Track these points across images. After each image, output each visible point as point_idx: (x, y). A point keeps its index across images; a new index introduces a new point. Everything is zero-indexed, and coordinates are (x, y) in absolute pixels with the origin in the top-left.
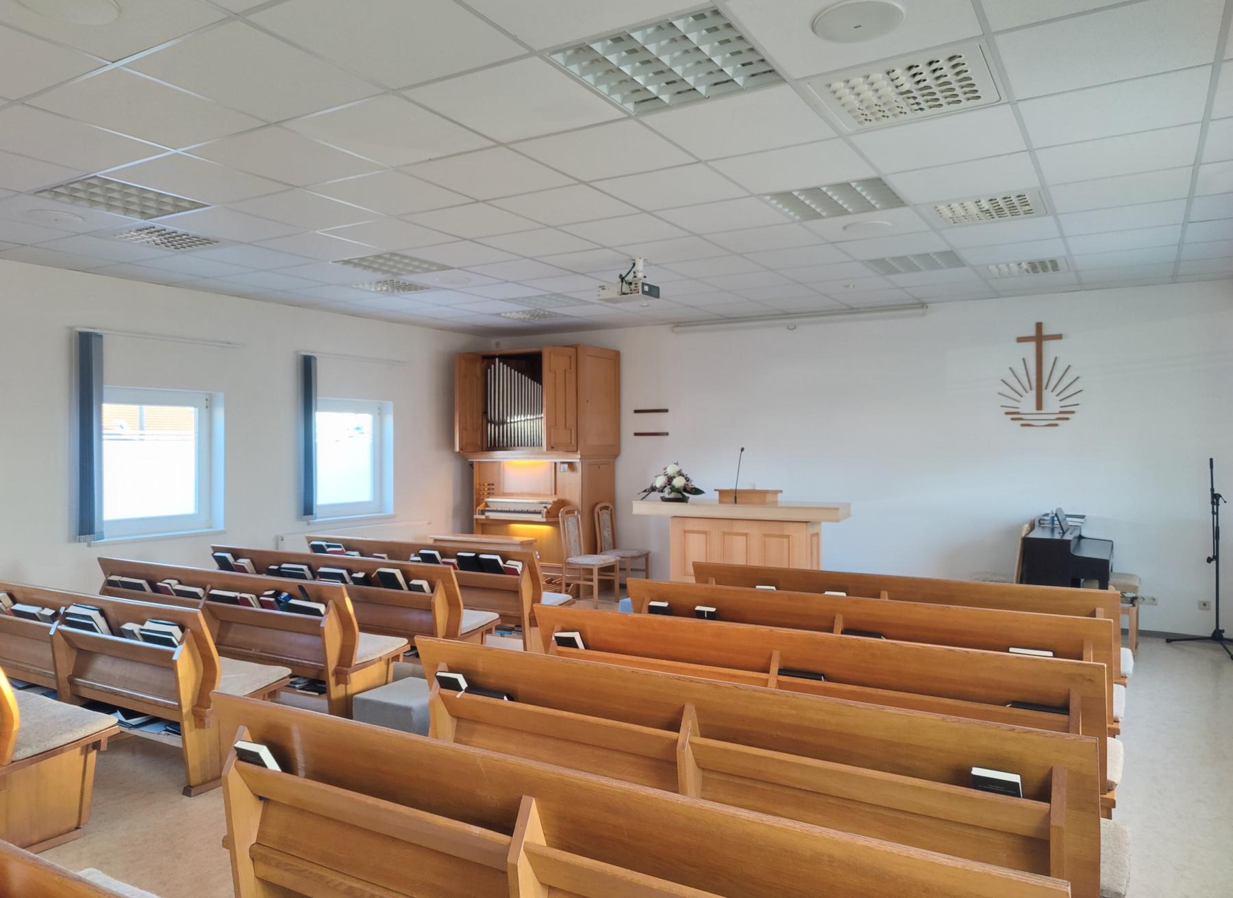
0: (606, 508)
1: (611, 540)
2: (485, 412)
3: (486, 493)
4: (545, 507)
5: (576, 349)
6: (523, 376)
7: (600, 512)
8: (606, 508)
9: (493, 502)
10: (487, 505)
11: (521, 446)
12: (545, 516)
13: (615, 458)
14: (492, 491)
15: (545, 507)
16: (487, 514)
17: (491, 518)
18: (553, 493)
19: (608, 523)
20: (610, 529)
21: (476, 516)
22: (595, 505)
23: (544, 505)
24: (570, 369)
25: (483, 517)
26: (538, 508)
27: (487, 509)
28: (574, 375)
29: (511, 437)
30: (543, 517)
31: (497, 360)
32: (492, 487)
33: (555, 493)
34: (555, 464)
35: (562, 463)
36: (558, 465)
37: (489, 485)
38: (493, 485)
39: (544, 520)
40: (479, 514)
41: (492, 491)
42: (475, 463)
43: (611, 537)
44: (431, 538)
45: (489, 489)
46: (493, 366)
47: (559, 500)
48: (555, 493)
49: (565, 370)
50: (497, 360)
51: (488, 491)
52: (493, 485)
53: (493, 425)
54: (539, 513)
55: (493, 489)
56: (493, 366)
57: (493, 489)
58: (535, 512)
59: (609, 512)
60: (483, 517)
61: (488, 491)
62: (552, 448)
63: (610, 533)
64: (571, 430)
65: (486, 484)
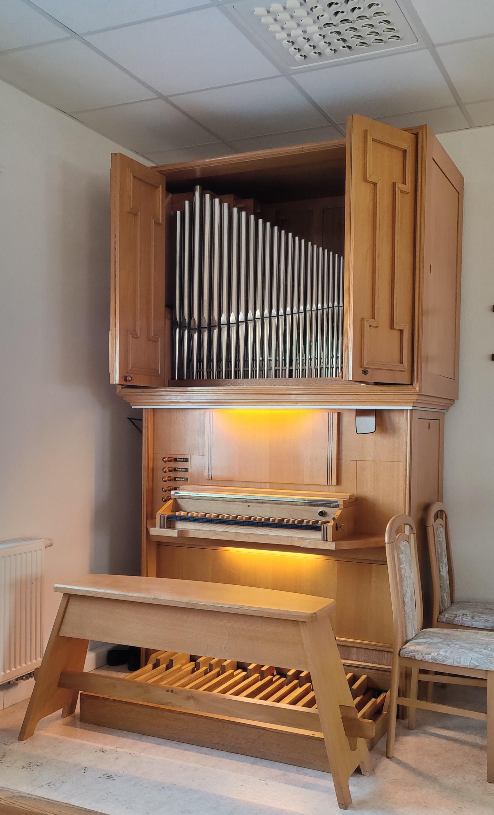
2: (170, 305)
4: (322, 514)
5: (417, 135)
9: (190, 498)
10: (177, 507)
11: (237, 376)
12: (330, 536)
13: (447, 408)
15: (322, 514)
16: (180, 525)
17: (192, 535)
18: (334, 482)
20: (445, 560)
21: (156, 531)
22: (426, 508)
23: (321, 509)
24: (404, 183)
25: (173, 533)
27: (177, 513)
30: (325, 539)
33: (339, 482)
34: (339, 414)
35: (360, 413)
36: (348, 419)
39: (331, 546)
40: (161, 527)
42: (144, 412)
44: (57, 590)
46: (187, 203)
47: (351, 497)
48: (339, 482)
49: (394, 184)
52: (187, 460)
53: (186, 332)
54: (315, 527)
56: (187, 203)
58: (300, 526)
59: (443, 523)
64: (402, 331)
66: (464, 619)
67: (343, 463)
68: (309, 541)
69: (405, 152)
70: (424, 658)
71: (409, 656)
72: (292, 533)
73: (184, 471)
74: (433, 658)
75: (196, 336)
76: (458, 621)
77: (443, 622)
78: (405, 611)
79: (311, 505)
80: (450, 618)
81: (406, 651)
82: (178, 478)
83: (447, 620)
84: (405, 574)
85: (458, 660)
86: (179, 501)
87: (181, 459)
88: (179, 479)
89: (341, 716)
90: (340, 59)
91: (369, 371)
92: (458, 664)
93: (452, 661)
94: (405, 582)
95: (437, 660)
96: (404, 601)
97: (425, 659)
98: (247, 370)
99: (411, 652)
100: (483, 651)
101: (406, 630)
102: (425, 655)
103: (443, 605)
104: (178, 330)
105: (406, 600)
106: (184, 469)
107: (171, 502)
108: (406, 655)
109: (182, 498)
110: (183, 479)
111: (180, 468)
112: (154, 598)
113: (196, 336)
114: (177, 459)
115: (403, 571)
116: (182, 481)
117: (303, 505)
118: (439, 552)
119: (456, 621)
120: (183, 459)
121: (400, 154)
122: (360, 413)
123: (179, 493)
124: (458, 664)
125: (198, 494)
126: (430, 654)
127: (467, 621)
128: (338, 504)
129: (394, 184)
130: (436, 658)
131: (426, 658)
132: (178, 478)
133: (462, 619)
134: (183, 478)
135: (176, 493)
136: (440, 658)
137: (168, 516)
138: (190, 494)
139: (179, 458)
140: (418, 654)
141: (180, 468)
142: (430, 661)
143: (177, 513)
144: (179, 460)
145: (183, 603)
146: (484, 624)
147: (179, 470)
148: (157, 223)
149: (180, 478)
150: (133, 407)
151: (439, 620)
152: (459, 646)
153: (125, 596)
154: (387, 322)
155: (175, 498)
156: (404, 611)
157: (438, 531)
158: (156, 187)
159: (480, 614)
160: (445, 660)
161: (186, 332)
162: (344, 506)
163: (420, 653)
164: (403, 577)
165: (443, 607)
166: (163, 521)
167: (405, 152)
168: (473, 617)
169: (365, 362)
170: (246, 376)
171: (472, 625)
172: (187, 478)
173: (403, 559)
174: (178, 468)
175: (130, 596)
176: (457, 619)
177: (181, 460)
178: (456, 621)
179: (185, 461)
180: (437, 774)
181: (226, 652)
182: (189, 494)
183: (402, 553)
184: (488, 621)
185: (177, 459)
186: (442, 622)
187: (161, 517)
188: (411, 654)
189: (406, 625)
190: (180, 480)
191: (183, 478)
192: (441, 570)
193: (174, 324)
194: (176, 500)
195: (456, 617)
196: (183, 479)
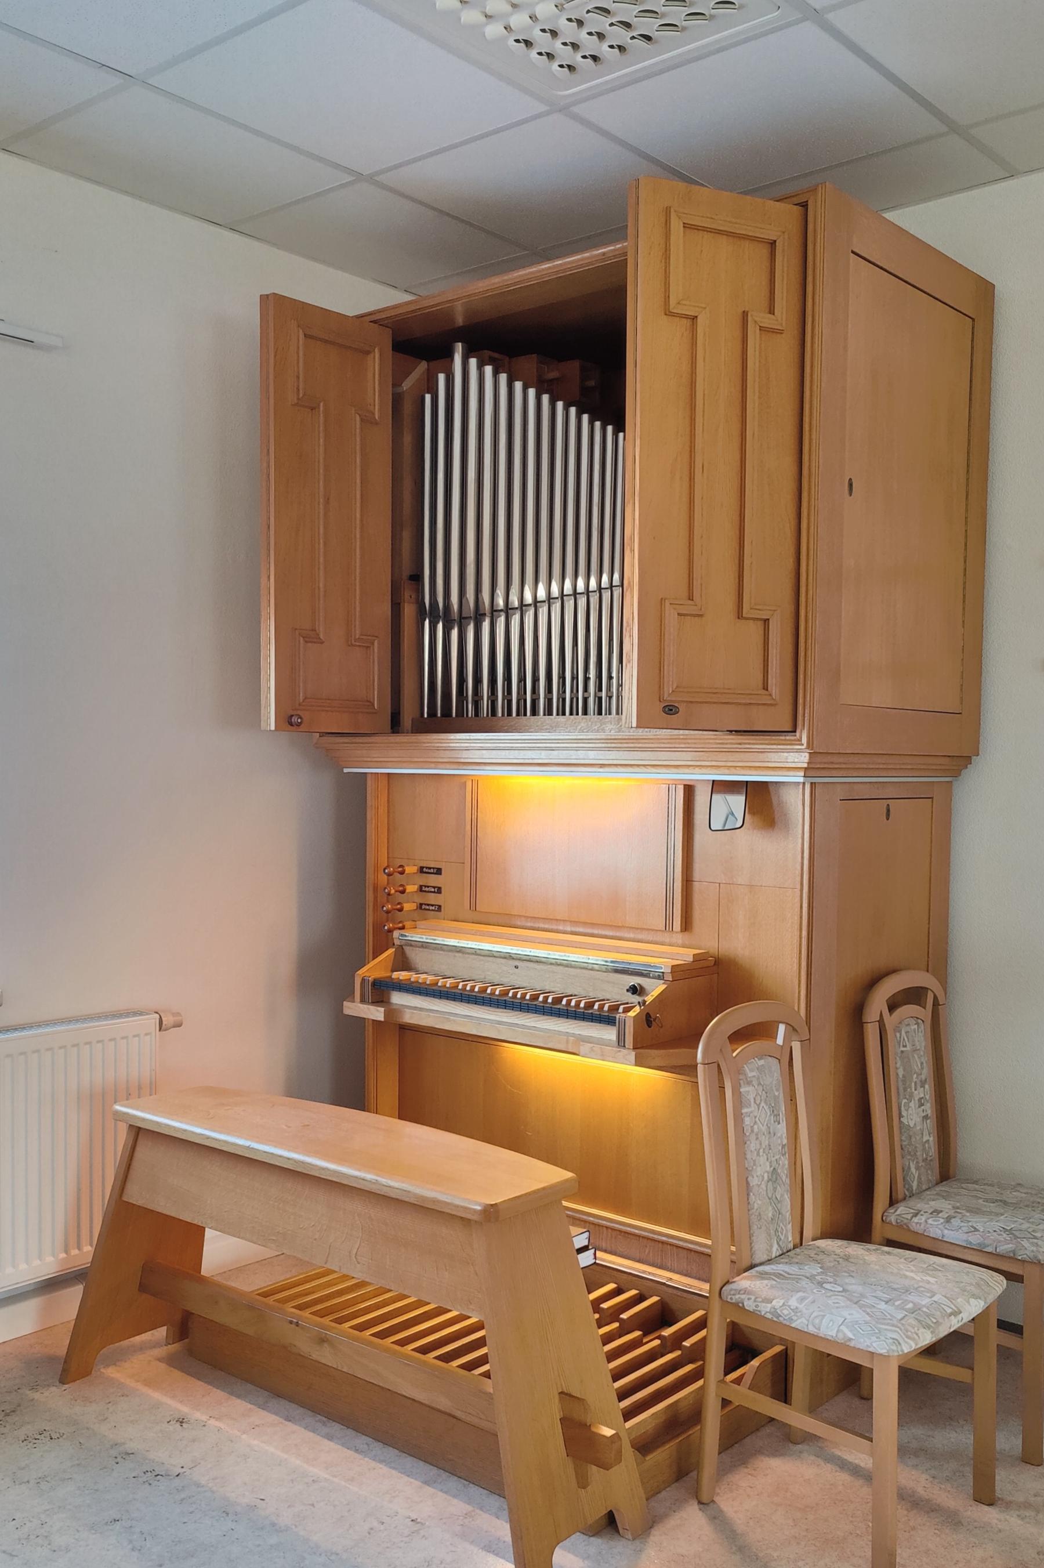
0: (914, 996)
1: (930, 1139)
3: (408, 907)
4: (634, 990)
5: (804, 205)
6: (560, 405)
7: (890, 1021)
8: (914, 996)
9: (424, 945)
10: (403, 963)
13: (957, 774)
14: (432, 899)
15: (634, 990)
16: (398, 999)
19: (921, 1064)
20: (926, 1092)
22: (873, 981)
25: (377, 1013)
26: (615, 990)
27: (395, 975)
28: (785, 348)
29: (522, 679)
31: (459, 347)
32: (433, 880)
33: (687, 925)
34: (689, 791)
35: (720, 787)
37: (421, 870)
38: (439, 871)
41: (432, 899)
42: (369, 777)
43: (931, 1124)
45: (421, 889)
46: (442, 377)
47: (697, 958)
48: (687, 925)
50: (459, 347)
51: (420, 899)
53: (440, 626)
55: (439, 890)
56: (442, 377)
57: (439, 890)
59: (926, 1013)
60: (377, 1013)
61: (420, 899)
62: (670, 710)
63: (929, 1108)
65: (410, 869)
66: (930, 1221)
67: (696, 886)
68: (592, 1045)
69: (773, 244)
70: (759, 1309)
71: (734, 1301)
72: (574, 1026)
73: (434, 892)
74: (774, 1312)
75: (455, 633)
76: (918, 1225)
77: (890, 1223)
78: (751, 1203)
79: (617, 971)
80: (903, 1216)
81: (731, 1290)
82: (425, 904)
83: (898, 1221)
84: (752, 1127)
85: (817, 1321)
86: (407, 949)
87: (430, 868)
88: (427, 907)
89: (558, 1416)
90: (646, 63)
91: (682, 708)
92: (816, 1331)
93: (806, 1322)
94: (752, 1145)
95: (781, 1316)
96: (748, 1183)
97: (759, 1311)
98: (550, 697)
99: (739, 1294)
100: (883, 1306)
101: (751, 1244)
102: (760, 1302)
103: (907, 1186)
104: (427, 623)
105: (754, 1181)
106: (434, 887)
107: (391, 951)
108: (729, 1297)
109: (411, 944)
110: (433, 908)
111: (428, 887)
112: (248, 1147)
113: (455, 633)
114: (424, 869)
115: (747, 1121)
116: (432, 910)
117: (604, 970)
118: (901, 1076)
119: (914, 1224)
120: (433, 868)
121: (765, 251)
122: (720, 787)
123: (406, 936)
124: (816, 1331)
125: (435, 940)
126: (770, 1301)
127: (934, 1228)
128: (663, 973)
129: (745, 314)
130: (779, 1312)
131: (762, 1309)
132: (425, 904)
133: (926, 1221)
134: (432, 905)
135: (402, 935)
136: (785, 1312)
137: (375, 980)
138: (423, 938)
139: (427, 868)
140: (749, 1299)
141: (428, 887)
142: (769, 1316)
143: (395, 975)
144: (427, 870)
145: (291, 1162)
146: (965, 1237)
147: (427, 889)
148: (368, 421)
149: (428, 905)
150: (346, 770)
151: (884, 1218)
152: (841, 1289)
153: (208, 1138)
154: (730, 604)
155: (401, 946)
156: (749, 1203)
157: (900, 1032)
158: (368, 353)
159: (968, 1214)
160: (793, 1318)
161: (440, 626)
162: (673, 978)
163: (753, 1298)
164: (747, 1134)
165: (908, 1190)
166: (366, 989)
167: (773, 244)
168: (948, 1220)
169: (668, 690)
170: (549, 712)
171: (943, 1236)
172: (440, 906)
173: (751, 1097)
174: (425, 886)
175: (214, 1139)
176: (915, 1220)
177: (429, 871)
178: (914, 1224)
179: (435, 874)
180: (775, 1555)
181: (359, 1263)
182: (421, 938)
183: (749, 1083)
184: (976, 1230)
185: (424, 869)
186: (888, 1223)
187: (363, 980)
188: (737, 1296)
189: (752, 1232)
190: (429, 910)
191: (432, 905)
192: (904, 1113)
193: (421, 614)
194: (403, 948)
195: (916, 1215)
196: (433, 908)
